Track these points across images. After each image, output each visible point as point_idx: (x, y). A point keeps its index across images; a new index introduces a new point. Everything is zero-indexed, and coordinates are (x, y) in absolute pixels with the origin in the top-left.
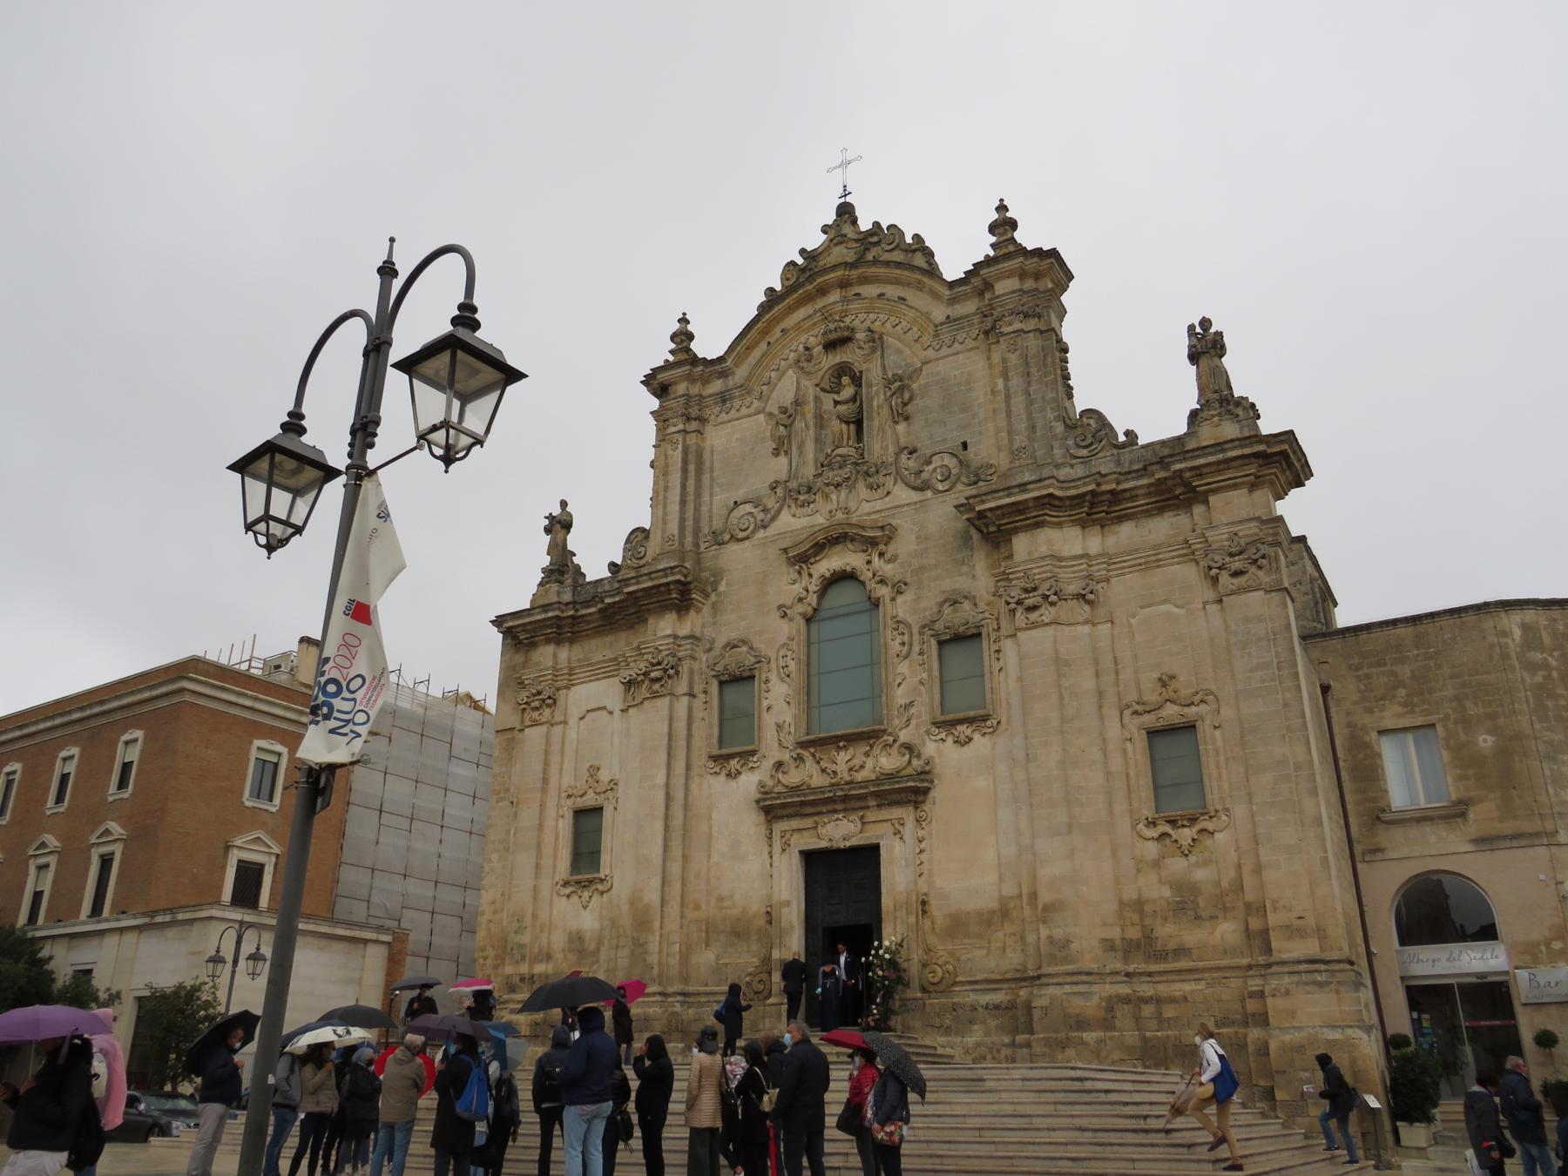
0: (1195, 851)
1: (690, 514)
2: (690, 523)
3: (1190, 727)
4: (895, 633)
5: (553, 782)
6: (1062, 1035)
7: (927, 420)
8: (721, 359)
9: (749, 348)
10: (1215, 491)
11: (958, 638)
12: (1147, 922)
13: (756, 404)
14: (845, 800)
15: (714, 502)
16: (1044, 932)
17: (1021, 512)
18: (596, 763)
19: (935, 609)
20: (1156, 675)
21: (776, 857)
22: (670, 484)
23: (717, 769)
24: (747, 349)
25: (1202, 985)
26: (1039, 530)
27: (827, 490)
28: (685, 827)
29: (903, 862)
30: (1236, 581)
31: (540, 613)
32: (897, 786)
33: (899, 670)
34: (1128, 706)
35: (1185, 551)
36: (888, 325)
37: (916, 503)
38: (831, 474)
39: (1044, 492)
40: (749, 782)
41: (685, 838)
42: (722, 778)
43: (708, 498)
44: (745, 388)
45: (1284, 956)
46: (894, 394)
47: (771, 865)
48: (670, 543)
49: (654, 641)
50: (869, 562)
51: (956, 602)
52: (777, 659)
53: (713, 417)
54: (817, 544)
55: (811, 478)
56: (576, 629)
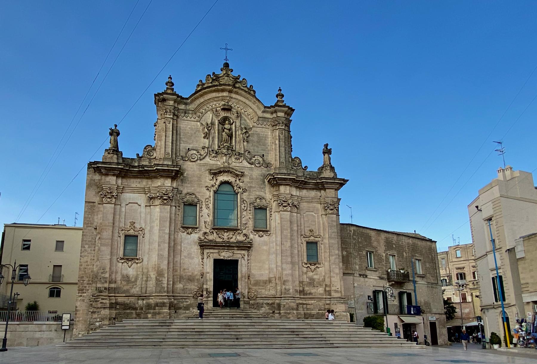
0: (315, 271)
1: (174, 147)
2: (174, 151)
3: (316, 243)
4: (242, 203)
5: (117, 224)
6: (289, 311)
7: (253, 145)
8: (187, 99)
9: (196, 99)
10: (328, 188)
11: (261, 208)
12: (304, 286)
13: (197, 118)
14: (228, 246)
16: (284, 287)
18: (134, 221)
19: (254, 199)
20: (309, 229)
21: (205, 260)
22: (167, 135)
23: (184, 231)
24: (195, 99)
25: (316, 301)
27: (223, 155)
29: (244, 266)
30: (331, 211)
31: (115, 165)
32: (245, 245)
33: (243, 214)
34: (303, 235)
36: (243, 111)
37: (249, 168)
38: (224, 151)
39: (293, 177)
40: (195, 236)
42: (185, 234)
43: (179, 144)
44: (195, 112)
45: (334, 297)
46: (244, 133)
47: (202, 261)
48: (168, 155)
49: (165, 187)
50: (236, 181)
51: (261, 199)
53: (181, 117)
55: (216, 149)
56: (126, 174)
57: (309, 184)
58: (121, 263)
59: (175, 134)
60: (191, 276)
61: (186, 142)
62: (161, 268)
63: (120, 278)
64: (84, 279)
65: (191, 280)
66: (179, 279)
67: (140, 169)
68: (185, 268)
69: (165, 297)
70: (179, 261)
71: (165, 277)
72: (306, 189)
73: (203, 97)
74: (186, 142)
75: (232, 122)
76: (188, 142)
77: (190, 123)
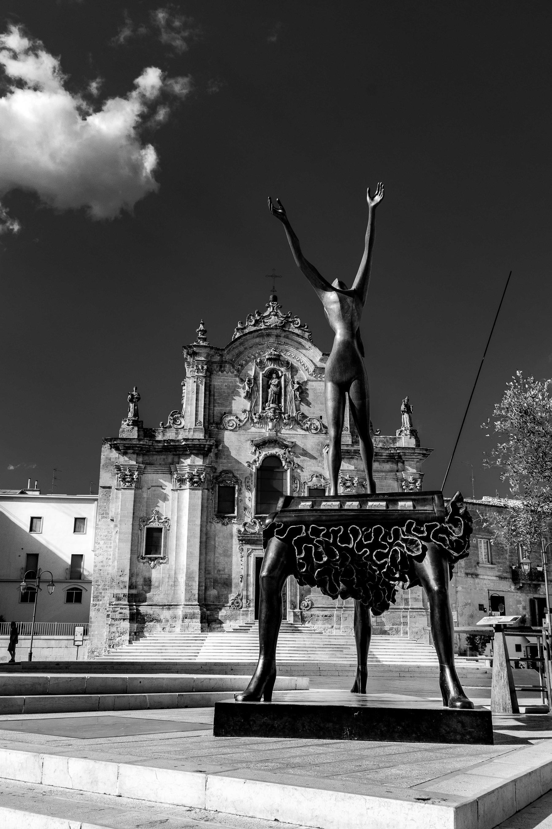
1: (207, 413)
10: (407, 460)
13: (235, 372)
15: (215, 410)
17: (348, 452)
19: (309, 477)
26: (351, 459)
28: (206, 542)
35: (394, 477)
41: (206, 548)
42: (220, 525)
52: (245, 482)
53: (215, 372)
54: (265, 441)
57: (381, 456)
58: (142, 564)
59: (208, 396)
60: (227, 579)
61: (221, 404)
62: (191, 570)
63: (141, 583)
64: (99, 583)
65: (227, 585)
66: (212, 584)
67: (165, 444)
68: (220, 569)
69: (195, 607)
70: (212, 560)
71: (195, 581)
72: (377, 461)
73: (244, 345)
74: (221, 404)
75: (280, 374)
76: (224, 405)
77: (226, 379)
